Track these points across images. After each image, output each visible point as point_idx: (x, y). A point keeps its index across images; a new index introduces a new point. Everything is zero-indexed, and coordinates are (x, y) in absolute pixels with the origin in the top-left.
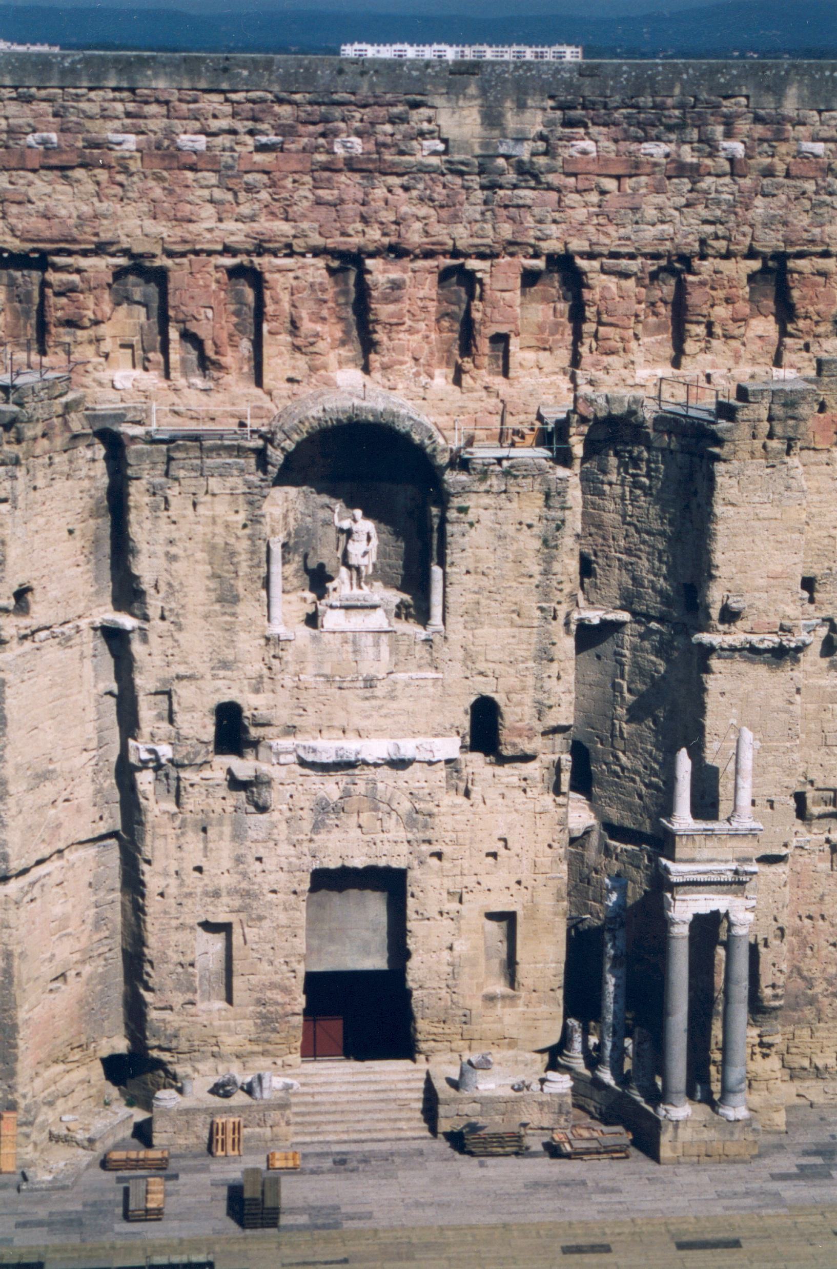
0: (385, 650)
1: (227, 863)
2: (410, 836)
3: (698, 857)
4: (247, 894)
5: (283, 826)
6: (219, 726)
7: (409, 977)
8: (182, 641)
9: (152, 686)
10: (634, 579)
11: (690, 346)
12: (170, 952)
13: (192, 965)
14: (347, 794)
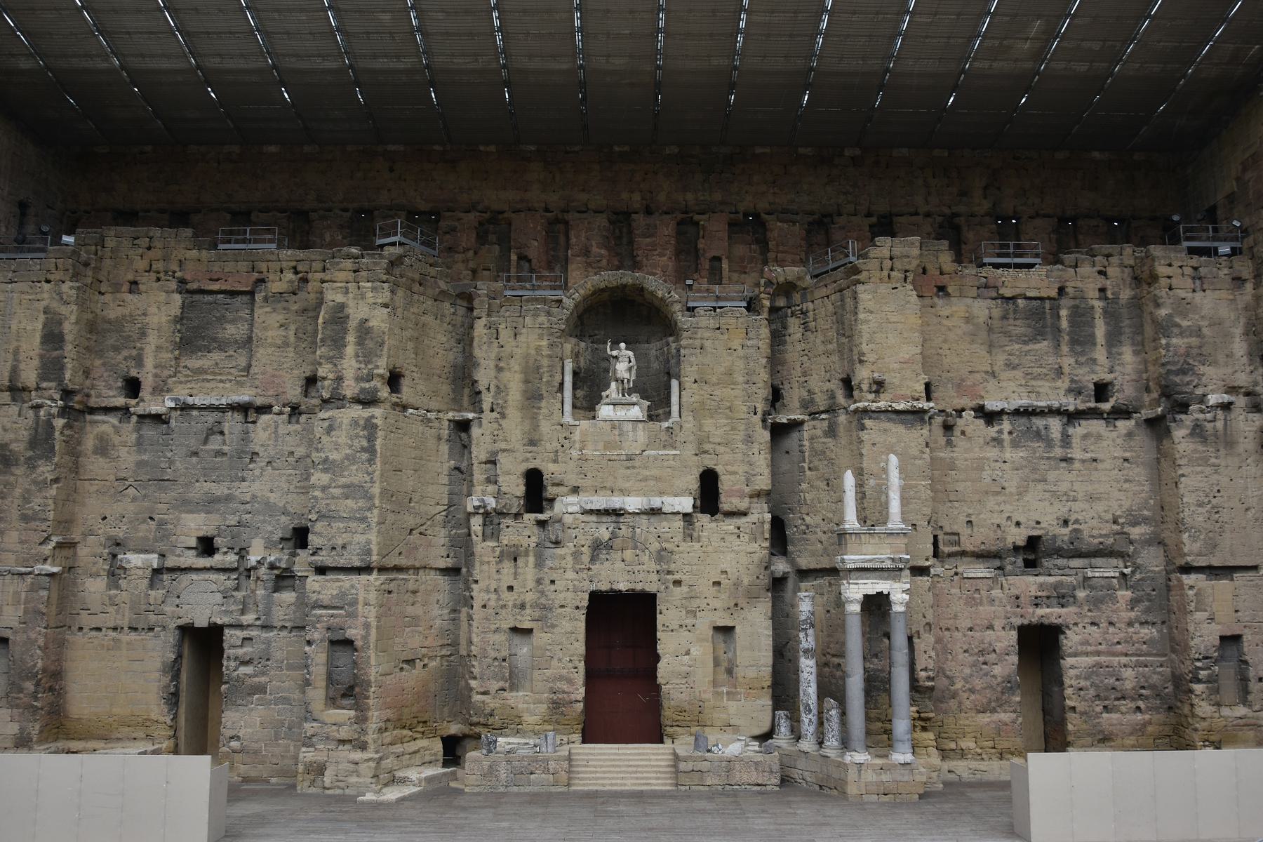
1: (531, 584)
2: (658, 568)
4: (544, 608)
5: (569, 558)
6: (528, 485)
7: (659, 675)
8: (504, 425)
9: (483, 457)
10: (809, 391)
12: (489, 649)
13: (504, 660)
14: (614, 536)
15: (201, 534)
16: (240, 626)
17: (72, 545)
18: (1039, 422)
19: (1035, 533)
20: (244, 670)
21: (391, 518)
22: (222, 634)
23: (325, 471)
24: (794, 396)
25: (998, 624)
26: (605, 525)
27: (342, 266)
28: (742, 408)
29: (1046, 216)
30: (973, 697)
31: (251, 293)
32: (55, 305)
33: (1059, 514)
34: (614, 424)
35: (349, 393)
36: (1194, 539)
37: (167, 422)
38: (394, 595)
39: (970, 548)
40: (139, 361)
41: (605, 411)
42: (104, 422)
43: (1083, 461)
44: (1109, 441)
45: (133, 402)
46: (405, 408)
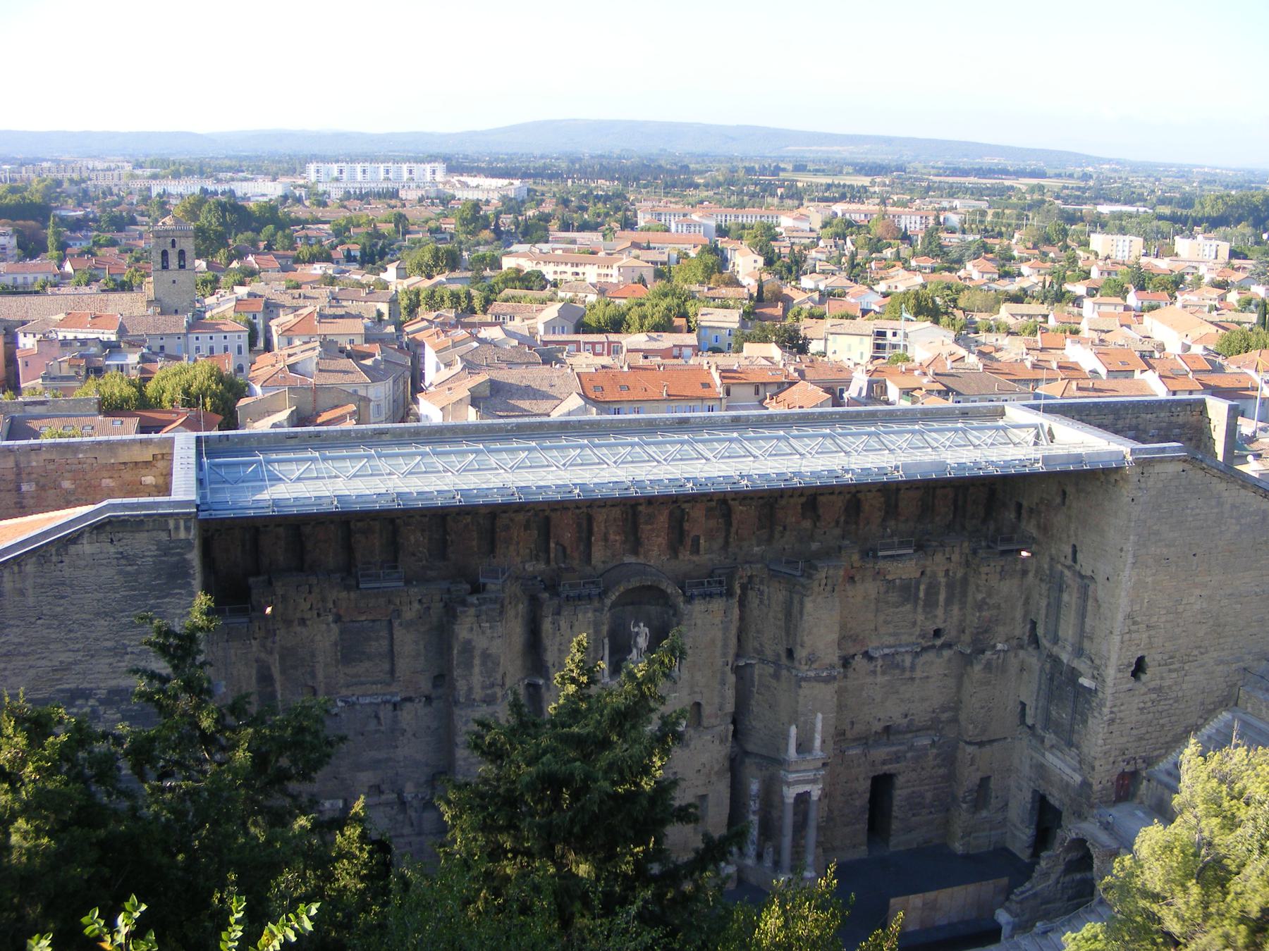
11: (777, 535)
16: (402, 836)
18: (898, 658)
24: (751, 644)
28: (719, 662)
29: (917, 488)
31: (390, 622)
32: (263, 655)
36: (976, 727)
44: (936, 665)
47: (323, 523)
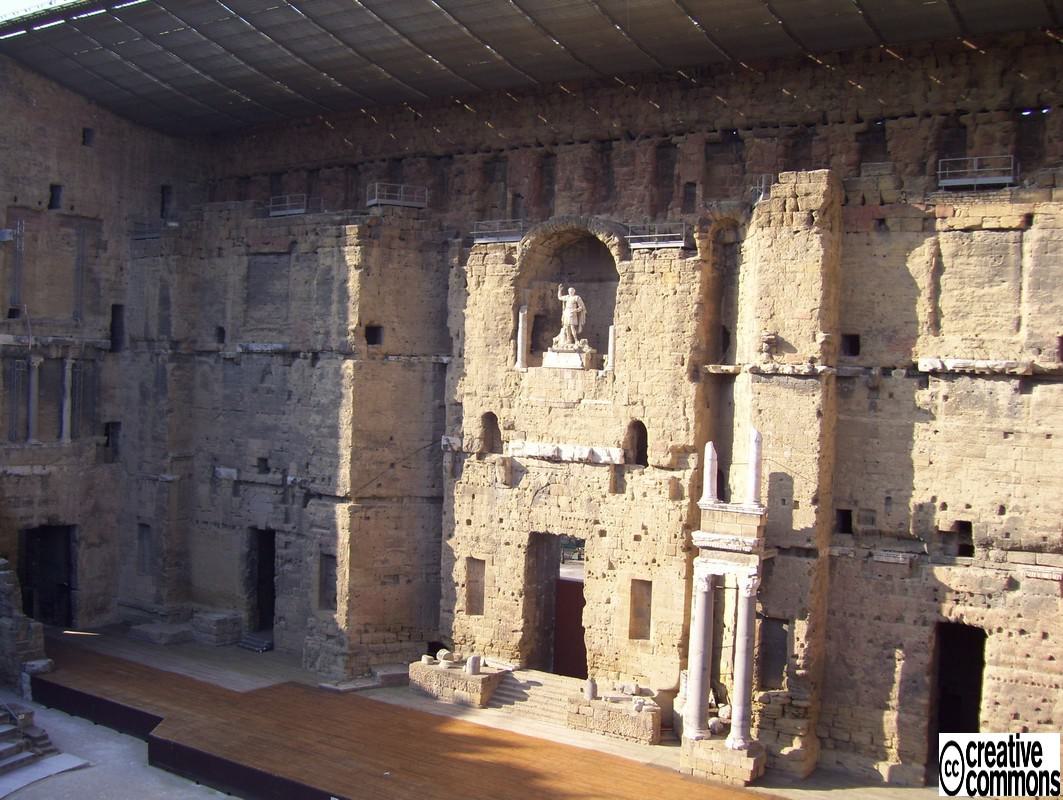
0: (579, 381)
1: (485, 521)
3: (717, 529)
7: (584, 617)
15: (260, 455)
16: (283, 532)
17: (188, 458)
19: (964, 518)
20: (288, 567)
21: (367, 455)
22: (274, 537)
23: (318, 413)
25: (909, 616)
26: (545, 470)
27: (328, 233)
28: (668, 359)
30: (872, 690)
33: (996, 498)
34: (557, 372)
35: (334, 345)
37: (238, 364)
38: (372, 521)
39: (886, 528)
40: (224, 317)
41: (549, 357)
42: (206, 362)
43: (1034, 436)
45: (221, 346)
46: (386, 356)
47: (297, 170)
